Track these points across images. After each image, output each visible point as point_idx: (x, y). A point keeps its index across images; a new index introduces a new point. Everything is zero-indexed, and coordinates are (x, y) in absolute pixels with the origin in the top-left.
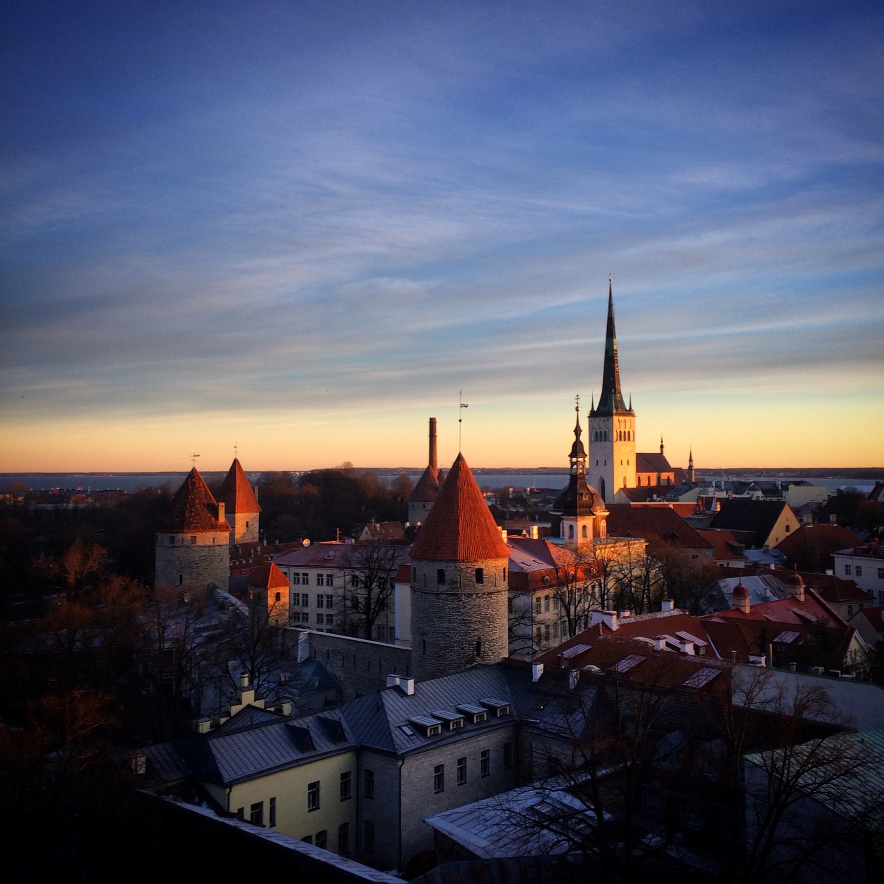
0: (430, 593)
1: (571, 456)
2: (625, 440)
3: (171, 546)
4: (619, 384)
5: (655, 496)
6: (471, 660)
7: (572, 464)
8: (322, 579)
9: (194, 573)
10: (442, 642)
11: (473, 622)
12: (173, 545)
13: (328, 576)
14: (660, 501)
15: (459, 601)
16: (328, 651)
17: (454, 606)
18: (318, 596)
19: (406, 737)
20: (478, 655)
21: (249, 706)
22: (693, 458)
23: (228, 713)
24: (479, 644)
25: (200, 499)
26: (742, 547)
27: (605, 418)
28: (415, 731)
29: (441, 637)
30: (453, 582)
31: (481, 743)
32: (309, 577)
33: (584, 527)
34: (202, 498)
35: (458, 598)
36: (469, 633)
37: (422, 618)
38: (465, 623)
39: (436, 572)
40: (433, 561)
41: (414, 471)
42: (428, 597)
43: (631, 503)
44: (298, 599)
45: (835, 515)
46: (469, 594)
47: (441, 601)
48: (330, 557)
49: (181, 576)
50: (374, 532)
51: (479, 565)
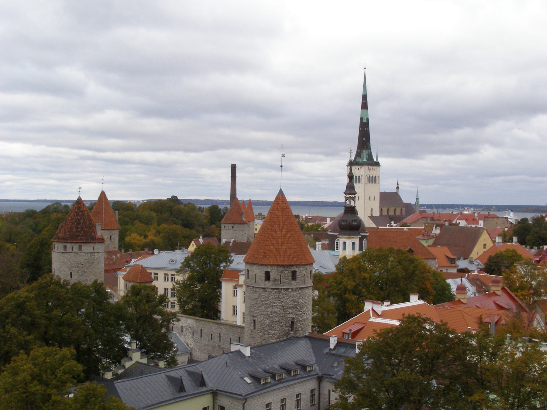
0: (259, 288)
1: (345, 193)
2: (372, 182)
3: (64, 252)
4: (370, 143)
6: (287, 333)
7: (346, 199)
8: (168, 277)
9: (81, 271)
10: (267, 321)
11: (289, 308)
12: (66, 251)
13: (172, 275)
15: (280, 293)
16: (182, 326)
17: (276, 297)
18: (165, 289)
19: (248, 385)
21: (137, 362)
23: (125, 367)
24: (292, 323)
25: (84, 219)
26: (454, 259)
27: (359, 167)
28: (253, 380)
29: (266, 318)
30: (275, 280)
31: (296, 389)
32: (158, 276)
33: (354, 243)
34: (85, 218)
35: (279, 291)
36: (286, 316)
37: (253, 305)
39: (264, 273)
40: (262, 265)
41: (223, 202)
42: (258, 290)
43: (379, 227)
44: (168, 293)
45: (517, 237)
46: (287, 289)
47: (267, 293)
49: (71, 274)
50: (197, 243)
51: (294, 269)
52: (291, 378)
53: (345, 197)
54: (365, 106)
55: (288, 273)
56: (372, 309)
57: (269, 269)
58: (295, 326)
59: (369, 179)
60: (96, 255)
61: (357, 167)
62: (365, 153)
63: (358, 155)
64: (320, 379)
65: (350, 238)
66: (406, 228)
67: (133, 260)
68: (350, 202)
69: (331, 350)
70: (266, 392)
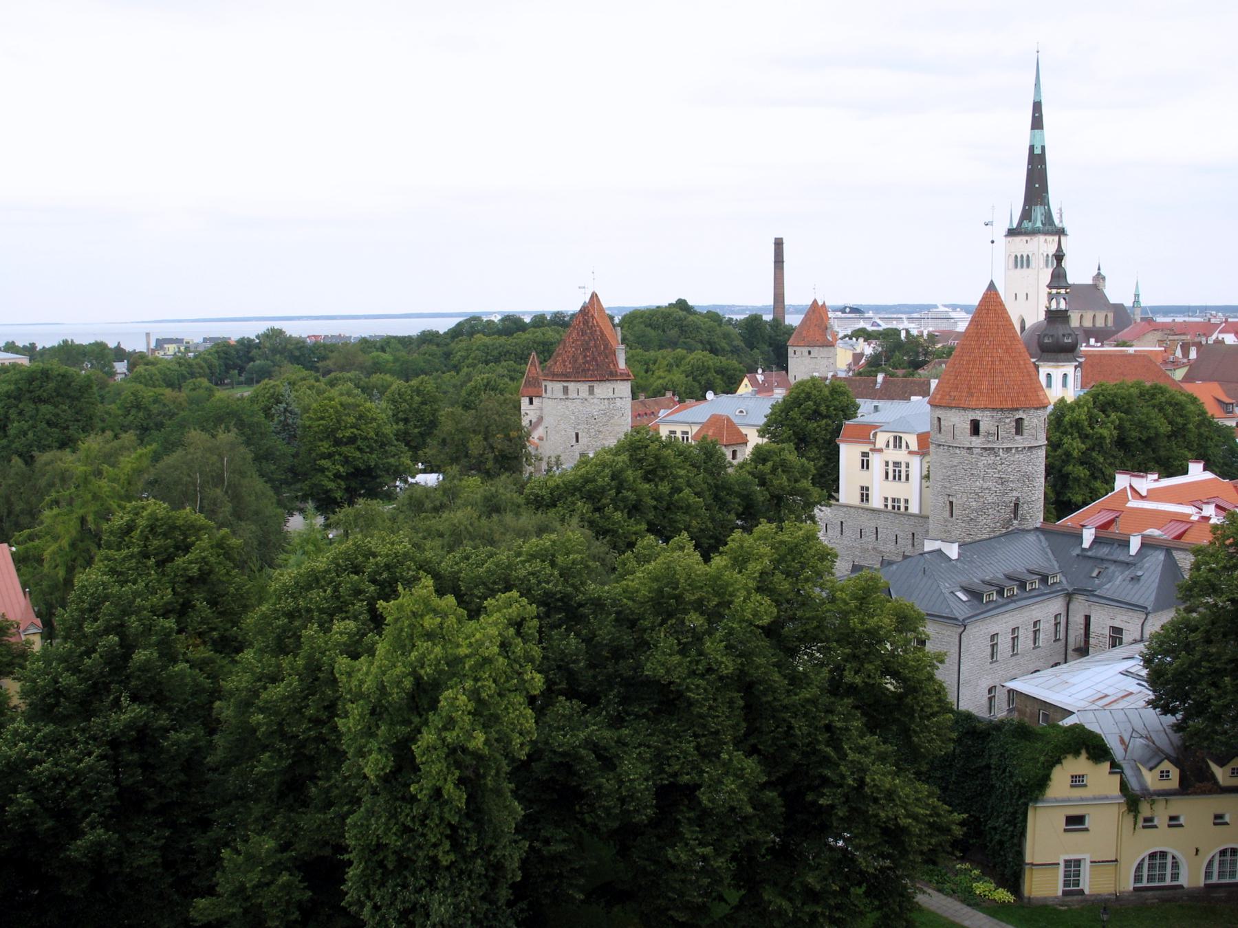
1: (1050, 287)
4: (1047, 192)
5: (1092, 341)
6: (1008, 523)
7: (1051, 297)
10: (974, 503)
14: (1102, 346)
17: (990, 462)
20: (1015, 518)
22: (1141, 293)
24: (1016, 505)
27: (1028, 238)
33: (1065, 375)
38: (1002, 481)
40: (964, 409)
42: (958, 451)
48: (741, 412)
49: (577, 435)
50: (754, 383)
52: (1026, 595)
53: (1050, 293)
54: (1037, 123)
55: (1009, 422)
56: (1131, 487)
57: (977, 415)
58: (1020, 512)
59: (1047, 261)
60: (619, 403)
61: (1025, 238)
62: (1038, 212)
63: (1026, 215)
64: (1069, 597)
65: (1057, 367)
66: (1131, 350)
67: (662, 413)
68: (1058, 303)
69: (1084, 550)
70: (992, 616)
